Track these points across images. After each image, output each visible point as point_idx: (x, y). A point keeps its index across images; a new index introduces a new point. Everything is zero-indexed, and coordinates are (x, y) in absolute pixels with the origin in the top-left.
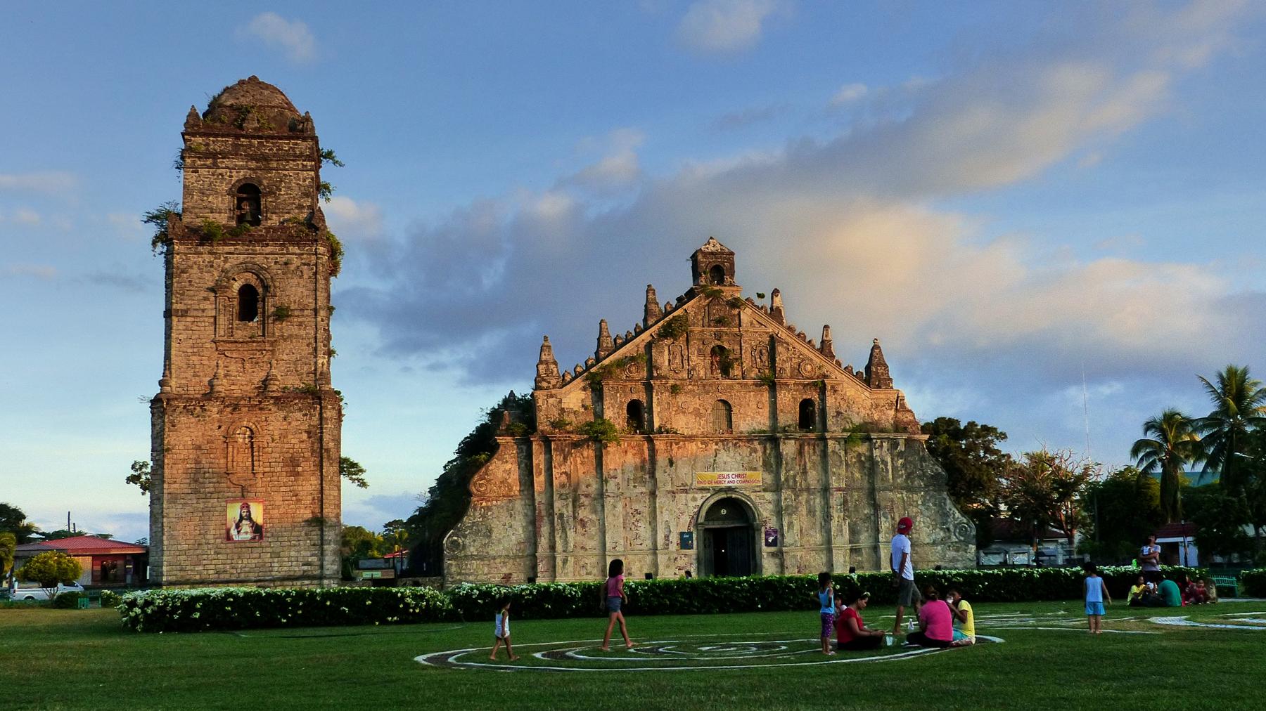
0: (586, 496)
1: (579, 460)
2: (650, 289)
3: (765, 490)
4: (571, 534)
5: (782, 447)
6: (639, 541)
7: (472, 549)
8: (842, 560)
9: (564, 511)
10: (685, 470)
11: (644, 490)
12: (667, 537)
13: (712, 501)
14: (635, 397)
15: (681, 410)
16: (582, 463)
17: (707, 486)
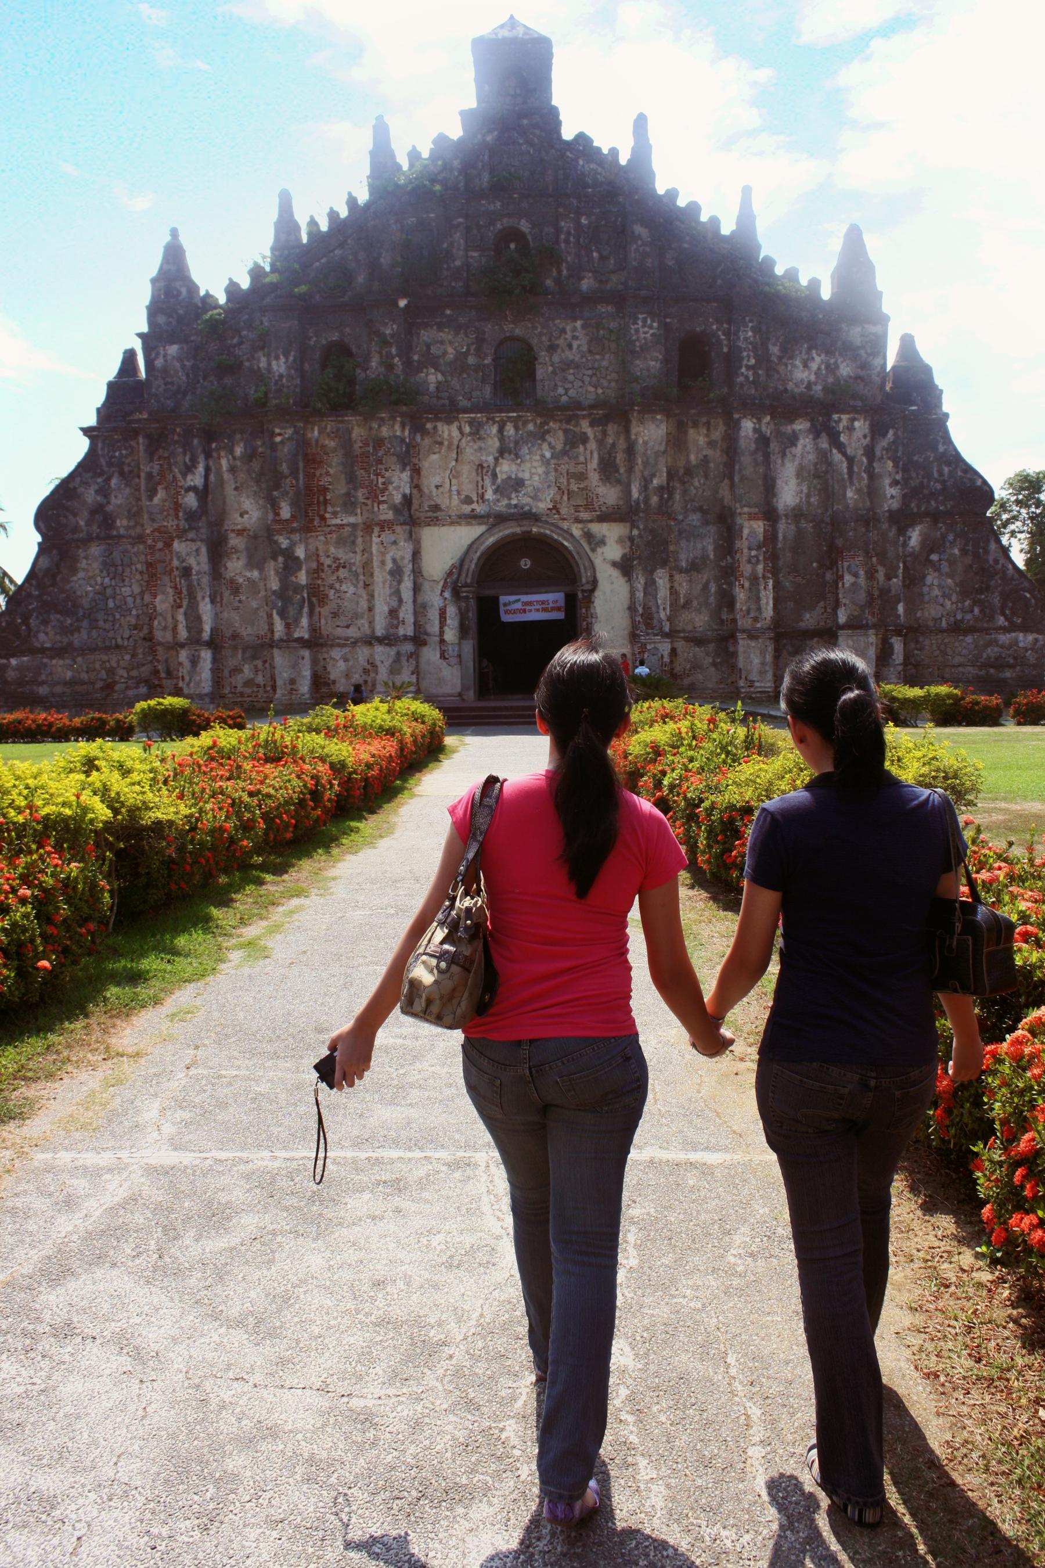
0: (240, 533)
1: (224, 462)
2: (381, 132)
3: (602, 518)
4: (206, 608)
5: (635, 428)
6: (343, 621)
7: (42, 636)
8: (756, 661)
9: (192, 561)
10: (436, 480)
11: (352, 520)
12: (393, 613)
13: (491, 540)
14: (335, 336)
15: (431, 361)
16: (232, 470)
17: (480, 509)
